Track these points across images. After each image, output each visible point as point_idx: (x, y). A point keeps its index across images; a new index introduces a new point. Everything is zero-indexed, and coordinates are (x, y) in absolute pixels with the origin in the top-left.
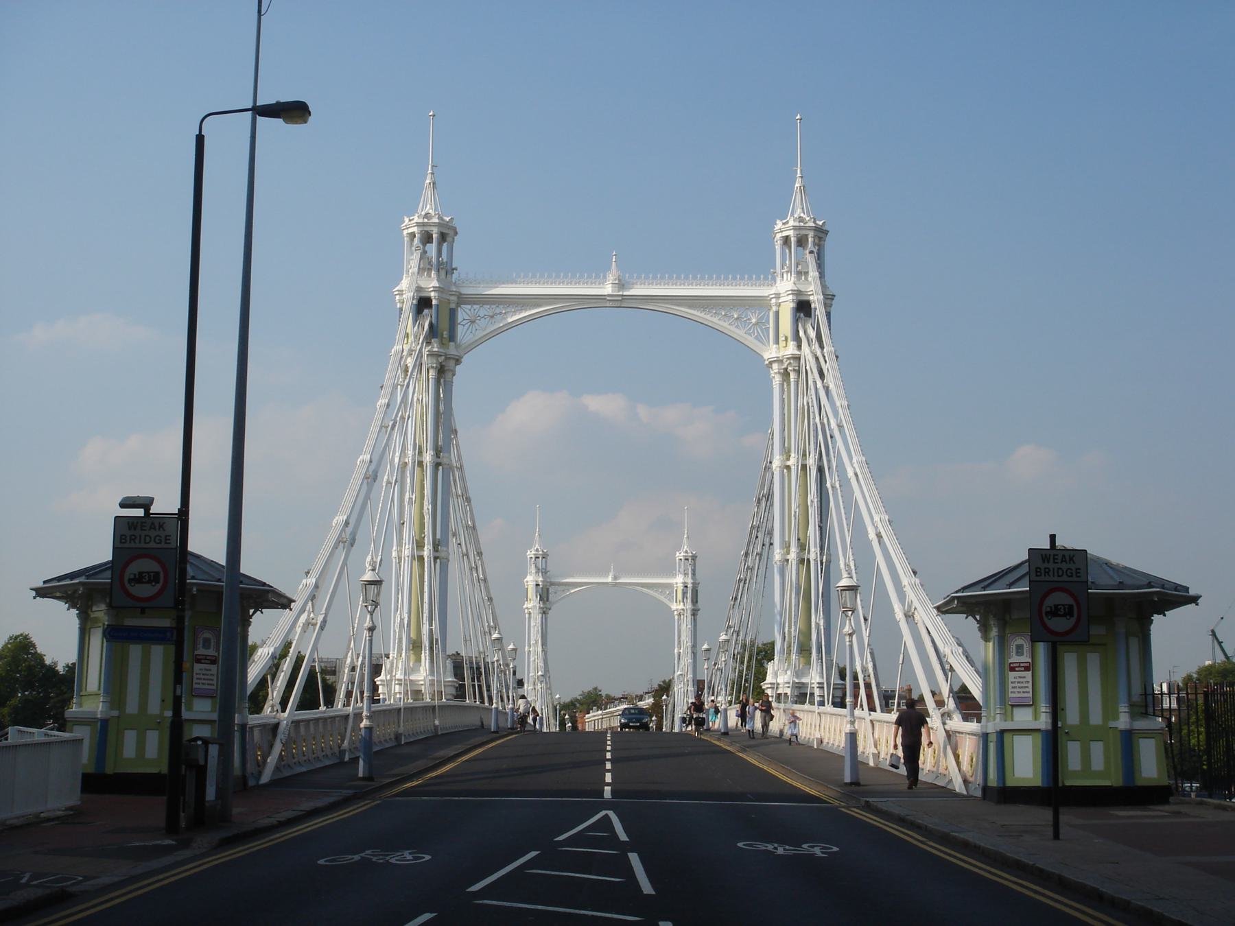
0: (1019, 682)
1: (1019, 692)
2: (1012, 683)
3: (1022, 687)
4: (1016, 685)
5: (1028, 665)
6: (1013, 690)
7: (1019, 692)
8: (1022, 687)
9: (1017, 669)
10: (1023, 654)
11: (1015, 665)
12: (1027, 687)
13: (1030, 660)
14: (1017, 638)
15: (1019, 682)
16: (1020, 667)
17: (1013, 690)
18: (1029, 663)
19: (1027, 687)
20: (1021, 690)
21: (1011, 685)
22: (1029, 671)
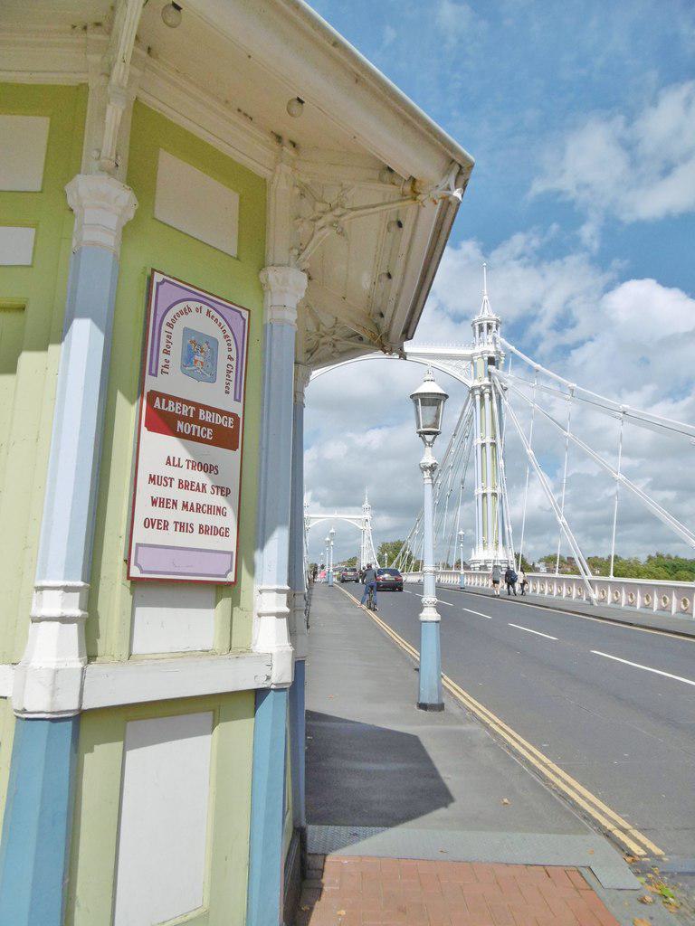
0: (184, 485)
1: (182, 527)
2: (152, 479)
3: (199, 508)
4: (173, 493)
5: (229, 423)
6: (159, 513)
7: (182, 527)
8: (199, 508)
9: (180, 425)
10: (213, 379)
11: (172, 407)
12: (220, 511)
13: (237, 408)
14: (193, 305)
15: (184, 485)
16: (195, 420)
17: (159, 513)
18: (234, 416)
19: (220, 511)
20: (197, 519)
21: (146, 491)
22: (234, 448)
